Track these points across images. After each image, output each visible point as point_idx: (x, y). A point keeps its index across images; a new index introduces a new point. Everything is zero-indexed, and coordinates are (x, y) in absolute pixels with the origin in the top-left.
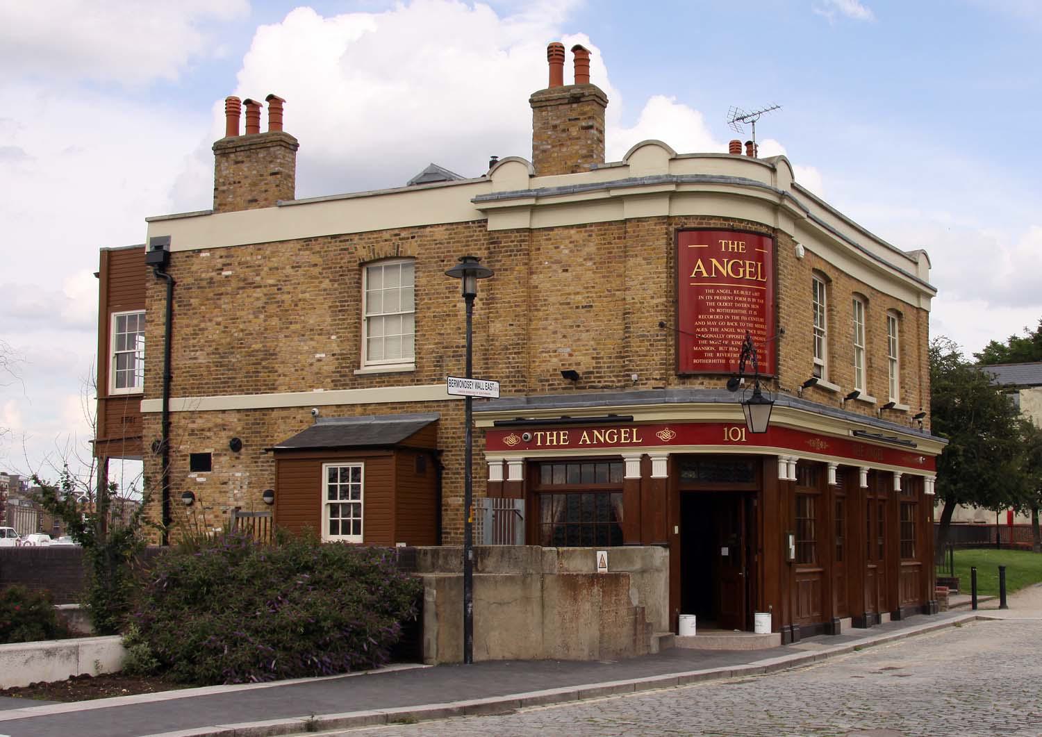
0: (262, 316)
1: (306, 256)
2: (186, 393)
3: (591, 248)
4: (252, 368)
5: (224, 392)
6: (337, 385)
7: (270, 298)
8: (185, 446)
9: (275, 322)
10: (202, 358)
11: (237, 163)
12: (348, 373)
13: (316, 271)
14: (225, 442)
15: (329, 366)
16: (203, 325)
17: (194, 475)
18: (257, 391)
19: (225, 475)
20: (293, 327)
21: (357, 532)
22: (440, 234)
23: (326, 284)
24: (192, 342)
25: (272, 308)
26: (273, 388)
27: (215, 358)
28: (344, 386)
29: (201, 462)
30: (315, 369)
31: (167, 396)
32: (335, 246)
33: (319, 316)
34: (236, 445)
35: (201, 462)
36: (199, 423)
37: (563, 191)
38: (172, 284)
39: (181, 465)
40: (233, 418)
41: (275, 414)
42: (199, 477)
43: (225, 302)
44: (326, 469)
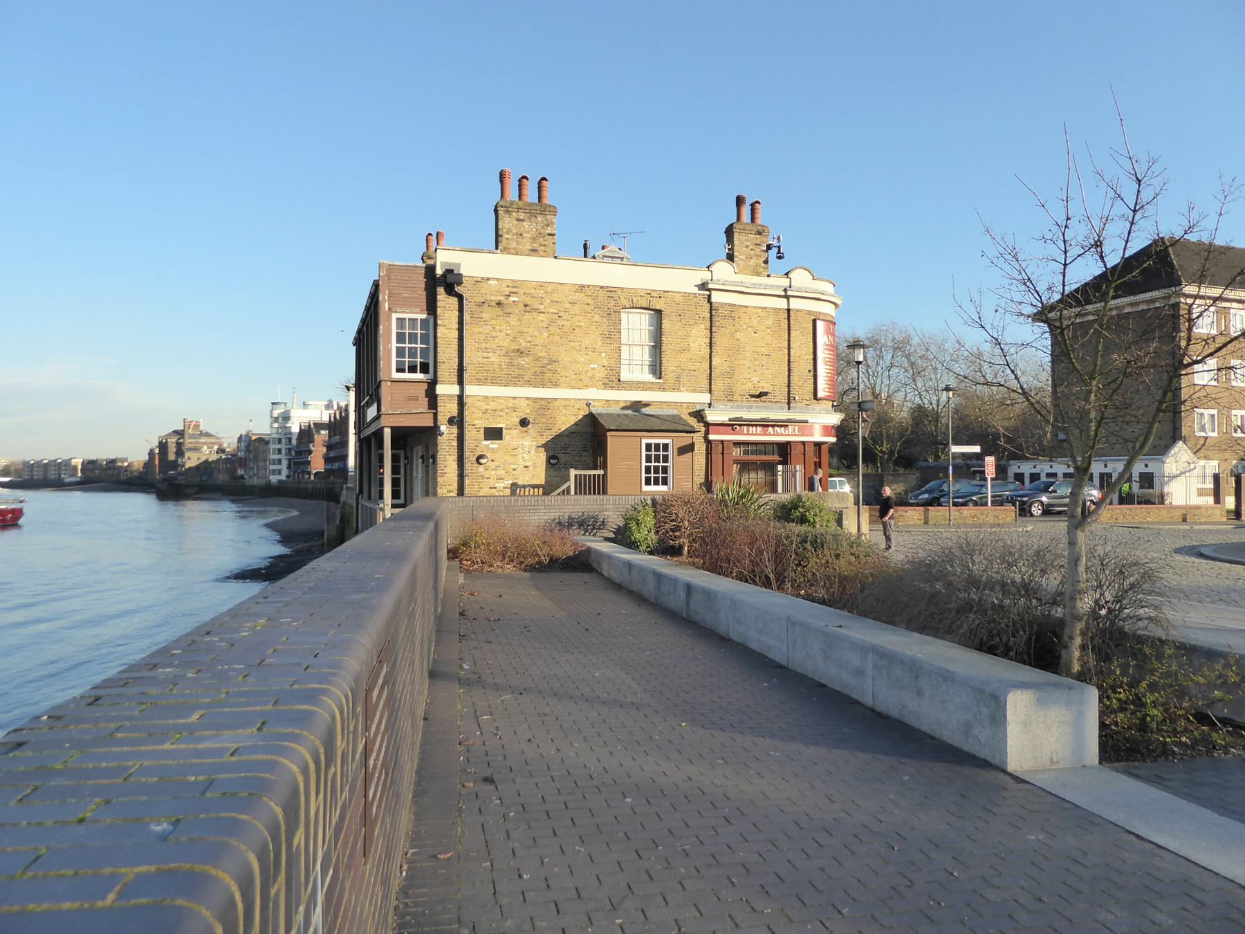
0: (546, 334)
1: (579, 296)
2: (479, 382)
3: (769, 322)
4: (538, 370)
5: (515, 385)
6: (606, 386)
7: (553, 321)
8: (476, 421)
9: (557, 338)
10: (494, 359)
11: (518, 220)
12: (614, 381)
13: (590, 308)
14: (517, 420)
15: (601, 373)
16: (494, 334)
17: (488, 442)
18: (543, 386)
19: (514, 443)
20: (572, 344)
21: (665, 482)
22: (678, 298)
23: (597, 318)
24: (484, 345)
25: (554, 329)
26: (555, 385)
27: (507, 359)
28: (612, 388)
29: (494, 434)
30: (590, 374)
31: (461, 382)
32: (602, 294)
33: (593, 338)
34: (524, 423)
35: (494, 434)
36: (492, 405)
37: (754, 285)
38: (460, 297)
39: (474, 437)
40: (524, 404)
41: (557, 403)
42: (493, 444)
43: (513, 320)
44: (644, 441)
